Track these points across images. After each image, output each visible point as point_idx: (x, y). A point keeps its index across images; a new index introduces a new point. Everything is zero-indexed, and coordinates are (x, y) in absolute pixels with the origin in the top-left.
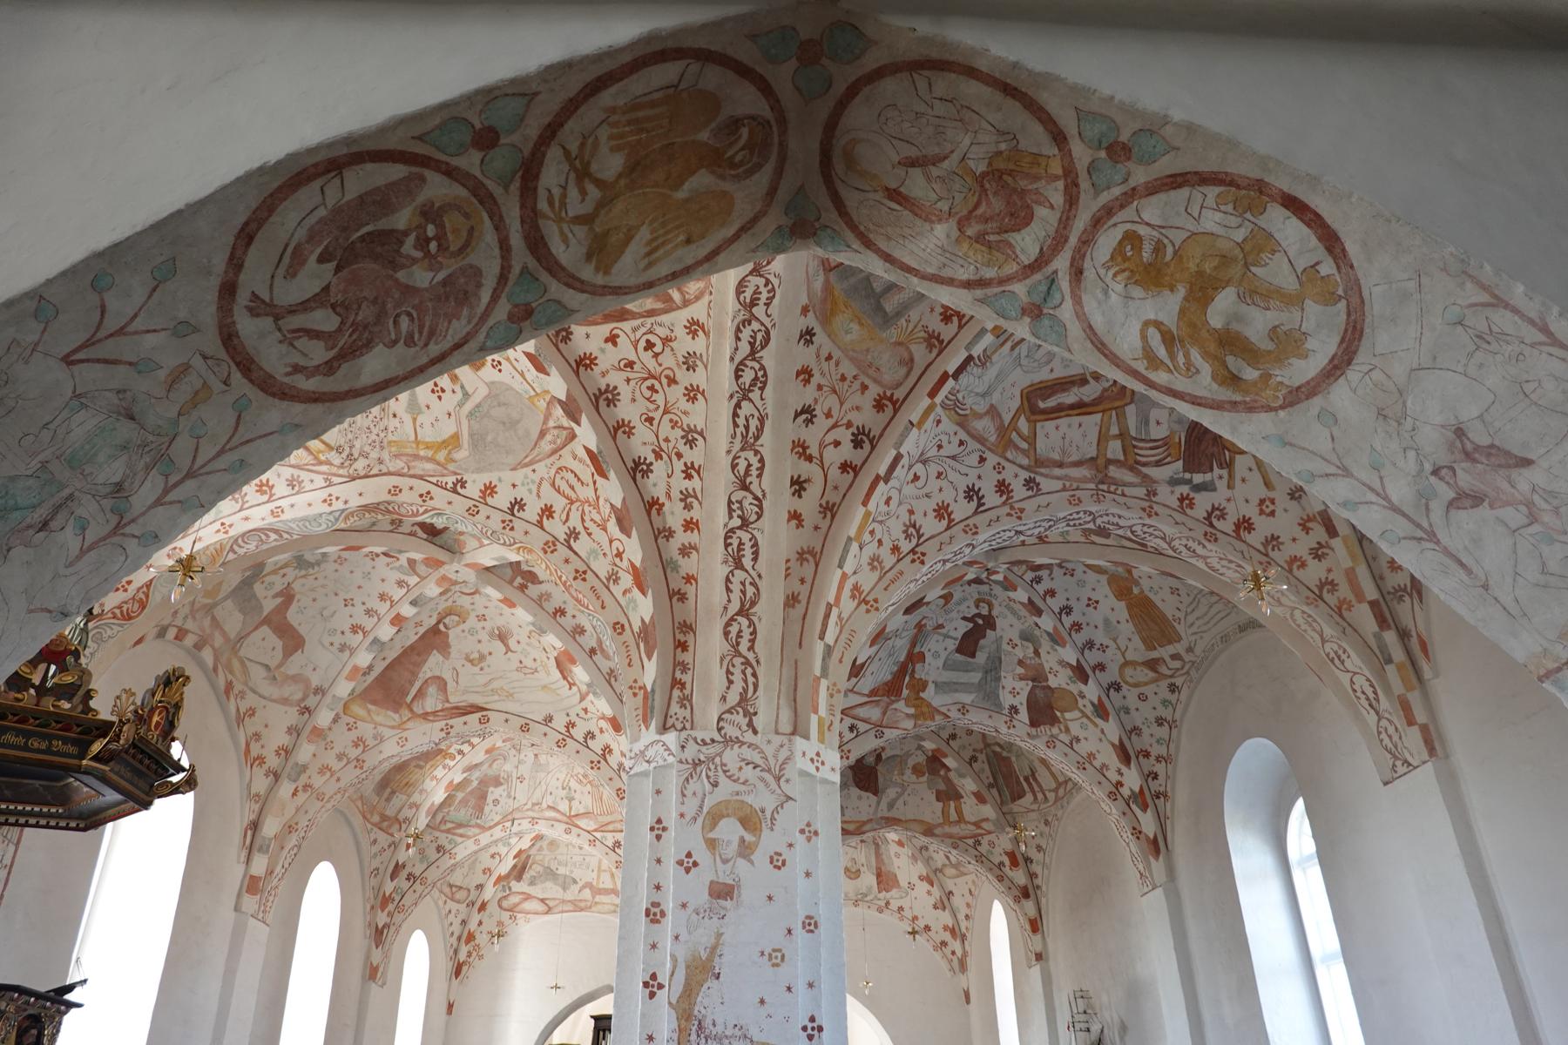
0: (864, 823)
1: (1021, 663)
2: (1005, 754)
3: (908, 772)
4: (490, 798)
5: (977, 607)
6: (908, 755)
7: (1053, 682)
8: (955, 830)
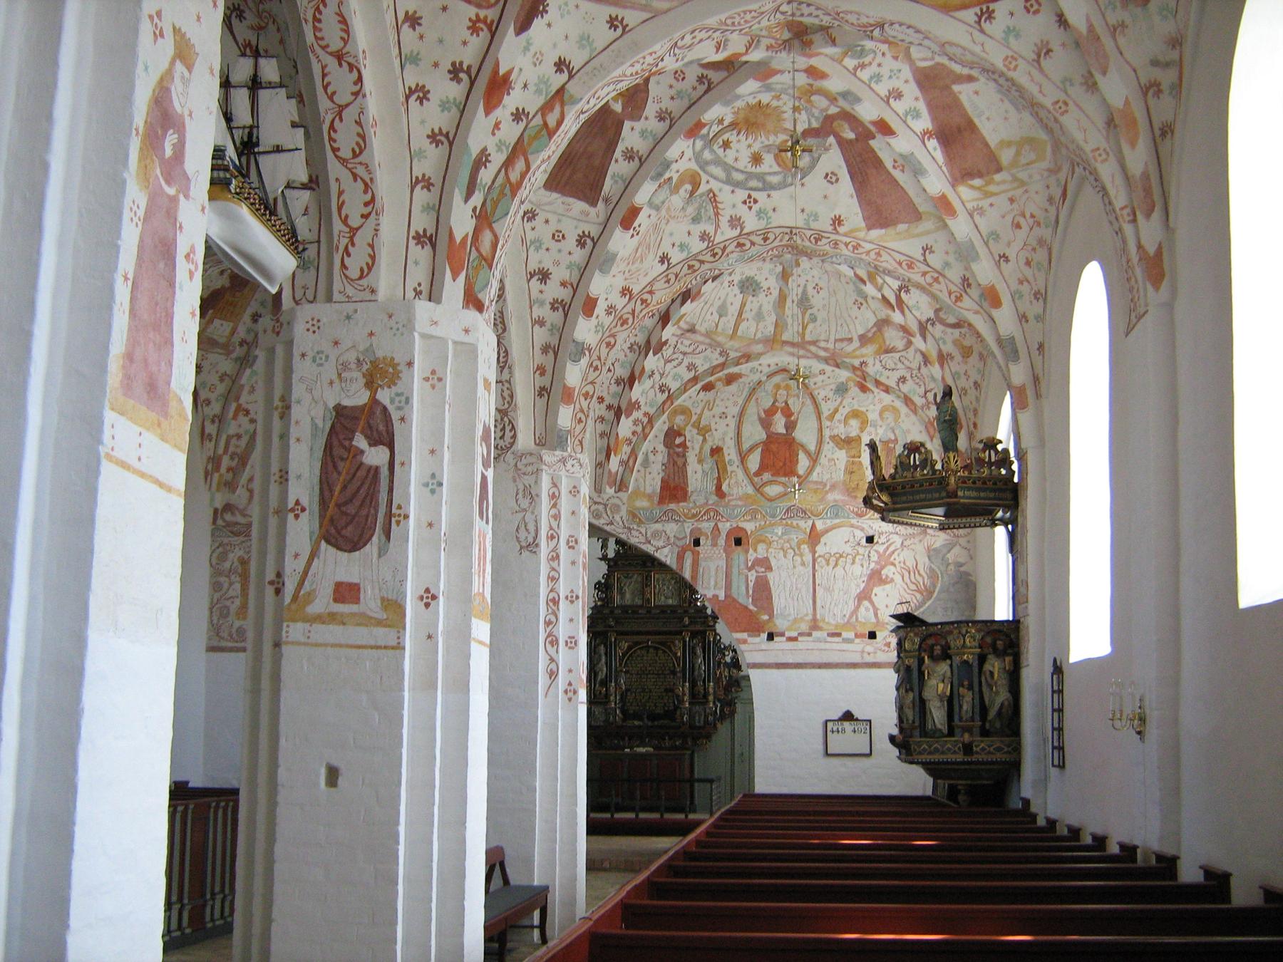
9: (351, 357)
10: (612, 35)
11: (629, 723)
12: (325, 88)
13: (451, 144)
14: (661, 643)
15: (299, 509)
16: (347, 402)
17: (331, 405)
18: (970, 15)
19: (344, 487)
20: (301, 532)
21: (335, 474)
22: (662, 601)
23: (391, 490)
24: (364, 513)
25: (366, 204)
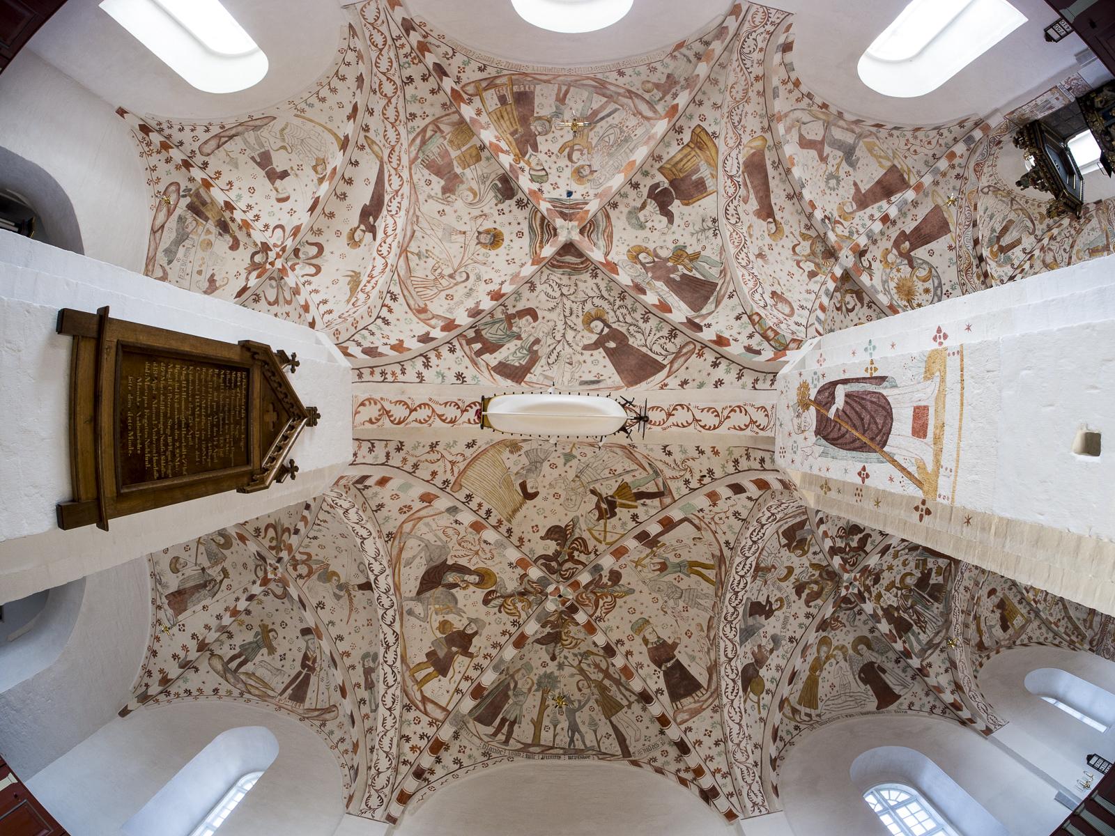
0: (399, 590)
1: (760, 646)
2: (510, 693)
3: (440, 618)
4: (434, 178)
5: (776, 601)
6: (459, 612)
7: (763, 672)
8: (410, 683)
9: (796, 421)
10: (735, 297)
12: (684, 426)
13: (744, 368)
15: (864, 475)
16: (814, 427)
17: (814, 439)
18: (716, 141)
19: (855, 427)
20: (881, 475)
21: (847, 436)
23: (857, 380)
24: (869, 406)
25: (741, 412)
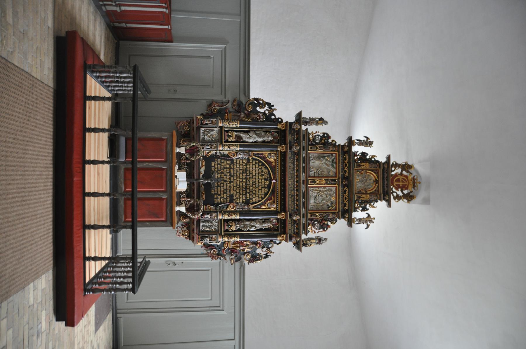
11: (203, 163)
14: (273, 191)
22: (312, 194)
